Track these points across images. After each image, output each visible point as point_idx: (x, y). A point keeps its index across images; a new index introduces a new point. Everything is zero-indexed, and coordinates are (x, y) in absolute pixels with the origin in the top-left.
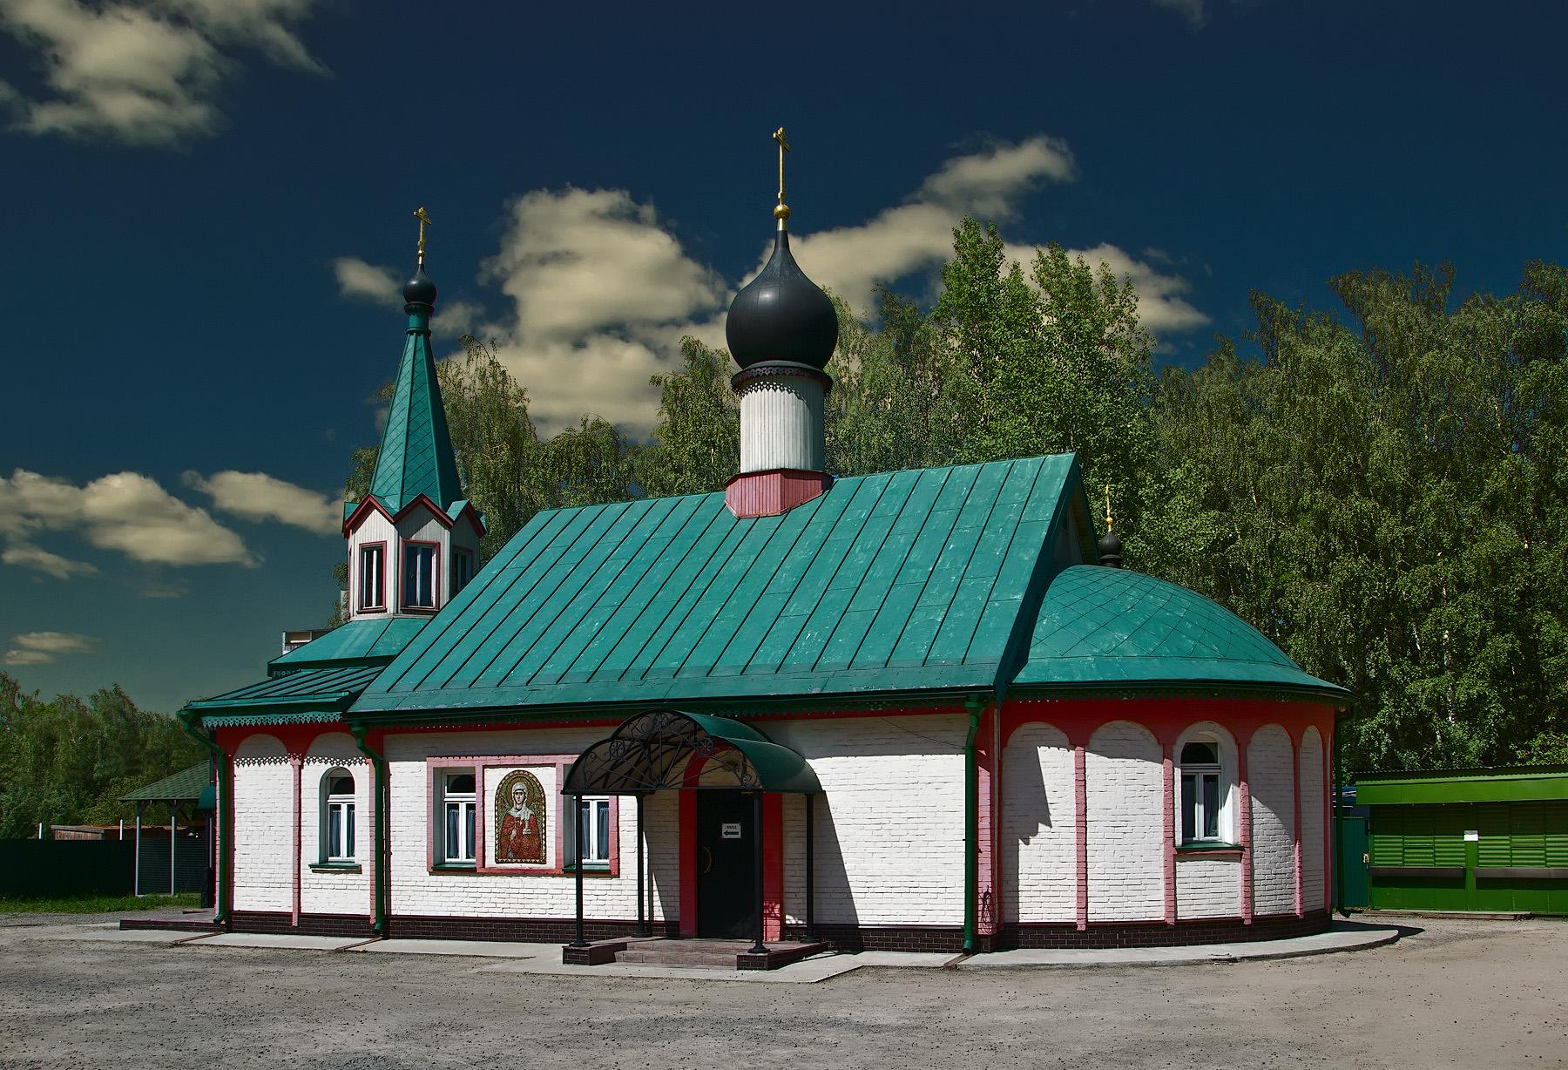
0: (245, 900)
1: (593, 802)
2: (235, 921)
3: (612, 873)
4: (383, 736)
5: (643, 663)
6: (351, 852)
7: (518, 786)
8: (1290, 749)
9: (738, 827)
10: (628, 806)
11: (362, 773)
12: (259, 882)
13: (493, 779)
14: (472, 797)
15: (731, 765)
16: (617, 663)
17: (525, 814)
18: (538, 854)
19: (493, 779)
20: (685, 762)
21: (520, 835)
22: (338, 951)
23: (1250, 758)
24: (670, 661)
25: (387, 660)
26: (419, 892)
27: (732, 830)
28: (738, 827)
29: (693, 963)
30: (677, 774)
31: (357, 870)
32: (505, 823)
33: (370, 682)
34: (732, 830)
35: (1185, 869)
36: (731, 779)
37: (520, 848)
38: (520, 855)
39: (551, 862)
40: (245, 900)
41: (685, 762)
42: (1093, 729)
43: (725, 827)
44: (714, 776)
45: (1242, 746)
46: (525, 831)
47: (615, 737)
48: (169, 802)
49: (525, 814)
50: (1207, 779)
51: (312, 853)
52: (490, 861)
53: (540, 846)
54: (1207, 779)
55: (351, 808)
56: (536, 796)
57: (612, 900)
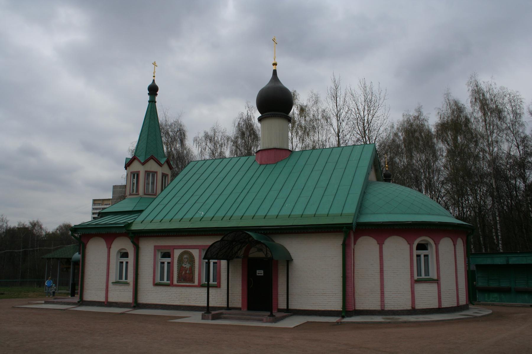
0: (89, 296)
1: (212, 262)
2: (82, 302)
3: (218, 286)
4: (137, 237)
5: (230, 214)
6: (126, 278)
7: (185, 256)
8: (453, 248)
9: (262, 272)
10: (224, 263)
11: (130, 250)
12: (94, 287)
13: (177, 253)
14: (169, 260)
15: (260, 250)
16: (221, 214)
17: (187, 266)
18: (192, 280)
19: (177, 253)
20: (244, 249)
21: (186, 273)
22: (121, 314)
23: (439, 249)
24: (239, 213)
25: (141, 211)
26: (150, 294)
27: (260, 273)
28: (262, 272)
29: (248, 320)
30: (242, 253)
31: (127, 284)
32: (181, 269)
33: (135, 219)
34: (260, 273)
35: (419, 287)
36: (261, 255)
37: (186, 278)
38: (185, 280)
39: (196, 283)
40: (89, 296)
41: (244, 249)
42: (386, 239)
43: (258, 271)
44: (254, 253)
45: (437, 245)
46: (188, 272)
47: (222, 240)
48: (58, 259)
49: (187, 266)
50: (425, 256)
51: (113, 277)
52: (175, 282)
53: (193, 277)
54: (425, 256)
55: (127, 263)
56: (192, 260)
57: (218, 298)
